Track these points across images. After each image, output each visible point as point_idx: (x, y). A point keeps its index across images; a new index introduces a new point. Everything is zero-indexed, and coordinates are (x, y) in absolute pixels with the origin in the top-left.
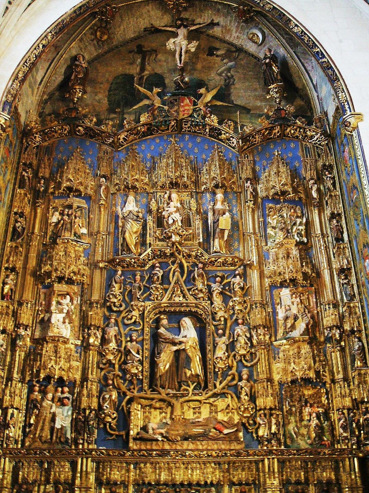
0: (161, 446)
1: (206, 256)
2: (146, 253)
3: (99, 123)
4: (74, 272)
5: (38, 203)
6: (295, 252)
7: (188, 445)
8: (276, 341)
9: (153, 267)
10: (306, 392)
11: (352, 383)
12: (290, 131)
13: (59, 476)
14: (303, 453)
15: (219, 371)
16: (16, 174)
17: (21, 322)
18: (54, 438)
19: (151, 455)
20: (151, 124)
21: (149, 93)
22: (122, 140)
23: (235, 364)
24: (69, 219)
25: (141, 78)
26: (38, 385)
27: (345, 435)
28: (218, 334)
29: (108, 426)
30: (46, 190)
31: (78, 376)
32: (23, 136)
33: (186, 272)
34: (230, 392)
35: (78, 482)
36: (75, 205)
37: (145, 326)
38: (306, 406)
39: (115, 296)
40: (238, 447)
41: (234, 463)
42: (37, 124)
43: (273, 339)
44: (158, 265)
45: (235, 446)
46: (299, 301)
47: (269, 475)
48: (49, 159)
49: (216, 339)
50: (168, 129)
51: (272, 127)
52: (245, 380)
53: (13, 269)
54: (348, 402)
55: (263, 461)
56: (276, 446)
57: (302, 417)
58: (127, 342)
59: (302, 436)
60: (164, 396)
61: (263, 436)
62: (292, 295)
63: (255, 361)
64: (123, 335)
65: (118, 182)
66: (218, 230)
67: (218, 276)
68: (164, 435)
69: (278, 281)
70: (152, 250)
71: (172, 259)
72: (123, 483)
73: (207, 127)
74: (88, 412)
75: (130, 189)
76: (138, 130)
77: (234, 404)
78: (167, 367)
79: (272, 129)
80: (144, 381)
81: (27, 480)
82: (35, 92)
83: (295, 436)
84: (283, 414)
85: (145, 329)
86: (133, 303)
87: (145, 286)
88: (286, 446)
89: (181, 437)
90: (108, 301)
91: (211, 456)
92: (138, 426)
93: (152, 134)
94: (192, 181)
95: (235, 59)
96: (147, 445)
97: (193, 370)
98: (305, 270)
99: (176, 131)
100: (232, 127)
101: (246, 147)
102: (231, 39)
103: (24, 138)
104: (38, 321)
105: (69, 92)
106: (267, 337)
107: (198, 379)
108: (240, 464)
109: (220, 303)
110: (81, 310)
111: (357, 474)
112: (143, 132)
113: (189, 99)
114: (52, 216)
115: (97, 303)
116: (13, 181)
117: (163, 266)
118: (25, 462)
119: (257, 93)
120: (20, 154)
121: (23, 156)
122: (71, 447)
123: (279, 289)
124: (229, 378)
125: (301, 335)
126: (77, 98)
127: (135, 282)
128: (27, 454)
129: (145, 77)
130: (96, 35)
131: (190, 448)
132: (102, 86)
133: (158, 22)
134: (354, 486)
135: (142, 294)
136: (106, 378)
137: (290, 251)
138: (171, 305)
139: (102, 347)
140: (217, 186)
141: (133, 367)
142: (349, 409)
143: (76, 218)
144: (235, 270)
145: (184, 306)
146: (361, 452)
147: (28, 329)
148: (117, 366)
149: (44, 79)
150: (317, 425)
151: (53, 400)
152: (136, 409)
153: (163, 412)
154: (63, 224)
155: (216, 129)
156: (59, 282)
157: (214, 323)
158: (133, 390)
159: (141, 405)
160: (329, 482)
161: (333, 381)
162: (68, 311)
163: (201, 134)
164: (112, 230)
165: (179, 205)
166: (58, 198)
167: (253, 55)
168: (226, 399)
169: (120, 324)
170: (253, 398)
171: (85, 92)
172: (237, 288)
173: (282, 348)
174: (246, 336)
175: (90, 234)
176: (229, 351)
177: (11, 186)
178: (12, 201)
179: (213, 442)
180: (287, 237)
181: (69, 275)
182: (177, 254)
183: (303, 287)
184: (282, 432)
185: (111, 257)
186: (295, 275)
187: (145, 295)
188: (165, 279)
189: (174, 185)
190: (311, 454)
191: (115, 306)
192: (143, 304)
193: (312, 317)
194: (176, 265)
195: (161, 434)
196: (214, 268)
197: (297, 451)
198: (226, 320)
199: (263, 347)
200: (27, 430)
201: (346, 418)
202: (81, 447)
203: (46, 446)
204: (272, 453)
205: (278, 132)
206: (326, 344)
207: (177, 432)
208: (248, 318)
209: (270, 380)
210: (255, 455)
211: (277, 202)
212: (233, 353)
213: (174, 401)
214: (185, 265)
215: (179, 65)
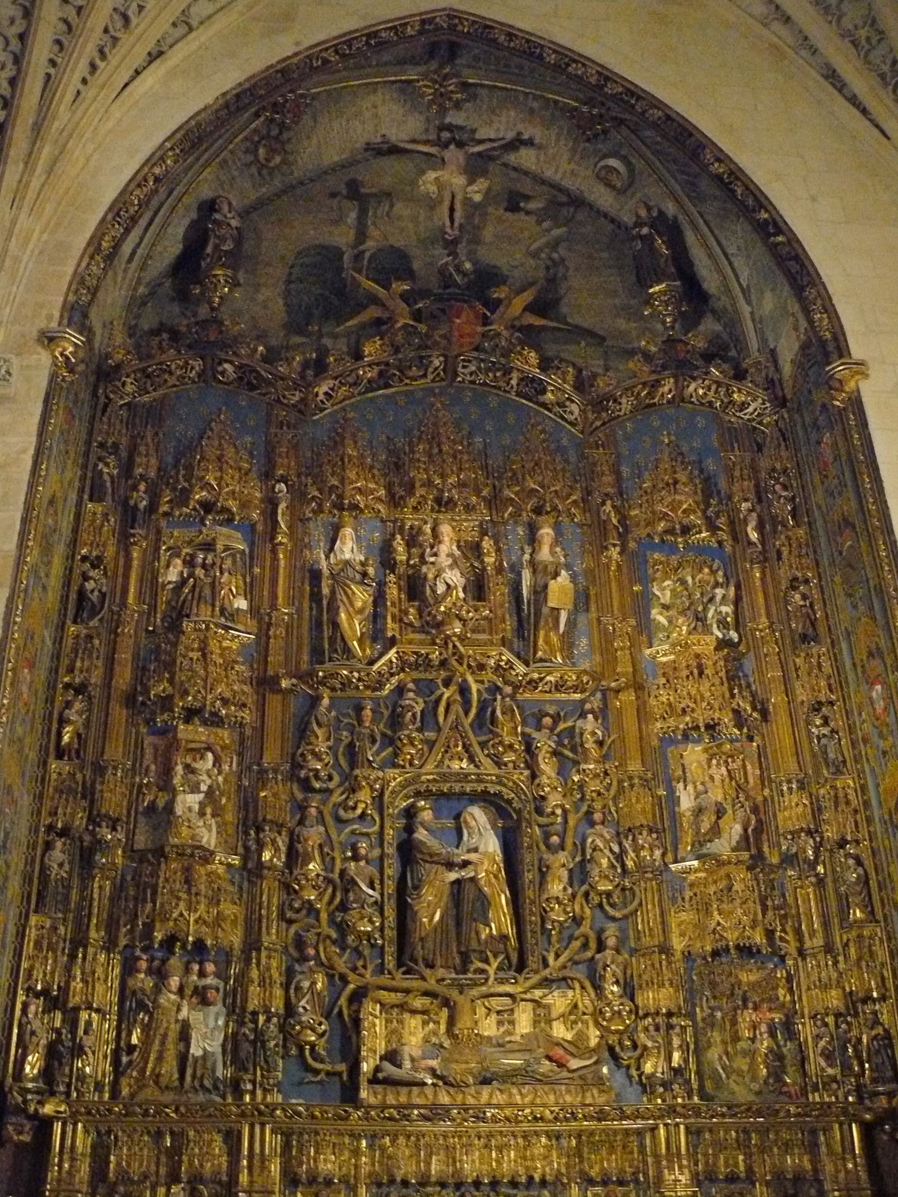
0: (430, 1097)
1: (521, 668)
2: (387, 657)
3: (271, 357)
4: (222, 699)
5: (133, 535)
6: (714, 662)
7: (491, 1096)
8: (676, 861)
9: (400, 690)
10: (744, 977)
11: (841, 958)
12: (695, 390)
13: (201, 1165)
14: (742, 1112)
15: (554, 929)
16: (85, 467)
17: (103, 811)
18: (188, 1078)
19: (407, 1117)
20: (387, 364)
21: (381, 292)
22: (321, 397)
23: (588, 911)
24: (206, 575)
25: (358, 257)
26: (145, 957)
27: (830, 1071)
28: (548, 846)
29: (307, 1053)
30: (152, 508)
31: (235, 939)
32: (98, 379)
33: (475, 704)
34: (578, 976)
35: (244, 1178)
36: (219, 547)
37: (387, 824)
38: (745, 1007)
39: (318, 757)
40: (601, 1100)
41: (592, 1134)
42: (129, 353)
43: (670, 857)
44: (411, 686)
45: (594, 1097)
46: (725, 773)
47: (668, 1161)
48: (157, 434)
49: (545, 856)
50: (425, 376)
51: (658, 381)
52: (612, 949)
53: (81, 689)
54: (834, 999)
55: (654, 1129)
56: (683, 1098)
57: (737, 1032)
58: (346, 859)
59: (739, 1075)
60: (431, 984)
61: (653, 1075)
62: (709, 760)
63: (631, 908)
64: (336, 845)
65: (316, 493)
66: (545, 611)
67: (547, 715)
68: (438, 1072)
69: (677, 728)
70: (397, 653)
71: (443, 674)
72: (344, 1180)
73: (515, 375)
74: (261, 1019)
75: (343, 509)
76: (358, 376)
77: (587, 1002)
78: (437, 917)
79: (656, 384)
80: (387, 949)
81: (127, 1173)
82: (119, 279)
83: (724, 1076)
84: (695, 1025)
85: (386, 831)
86: (357, 772)
87: (384, 735)
88: (703, 1096)
89: (474, 1077)
90: (302, 767)
91: (542, 1119)
92: (375, 1052)
93: (387, 386)
94: (484, 498)
95: (568, 221)
96: (398, 1093)
97: (493, 925)
98: (738, 705)
99: (442, 380)
100: (570, 378)
101: (598, 423)
102: (558, 177)
103: (102, 385)
104: (141, 809)
105: (200, 283)
106: (658, 853)
107: (505, 945)
108: (604, 1138)
109: (553, 775)
110: (239, 786)
111: (858, 1160)
112: (369, 381)
113: (472, 307)
114: (168, 566)
115: (275, 771)
116: (77, 484)
117: (426, 688)
118: (120, 1134)
119: (617, 301)
120: (93, 418)
121: (97, 425)
122: (224, 1097)
123: (681, 746)
124: (576, 944)
125: (734, 850)
126: (221, 298)
127: (359, 725)
128: (126, 1115)
129: (367, 255)
130: (256, 156)
131: (494, 1101)
132: (270, 270)
133: (394, 131)
134: (854, 1186)
135: (378, 753)
136: (300, 943)
137: (704, 661)
138: (444, 777)
139: (291, 873)
140: (538, 511)
141: (362, 918)
142: (838, 1015)
143: (222, 573)
144: (583, 702)
145: (469, 782)
146: (869, 1109)
147: (119, 828)
148: (324, 916)
149: (140, 251)
150: (771, 1050)
151: (181, 991)
152: (372, 1015)
153: (431, 1019)
154: (194, 586)
155: (533, 380)
156: (187, 721)
157: (542, 820)
158: (362, 971)
159: (381, 1005)
160: (798, 1178)
161: (801, 953)
162: (210, 787)
163: (499, 388)
164: (306, 605)
165: (457, 553)
166: (179, 525)
167: (606, 216)
168: (570, 993)
169: (329, 819)
170: (629, 991)
171: (235, 284)
172: (590, 745)
173: (692, 877)
174: (611, 850)
175: (254, 610)
176: (575, 883)
177: (73, 497)
178: (75, 530)
179: (546, 1088)
180: (695, 628)
181: (213, 704)
182: (455, 663)
183: (732, 741)
184: (693, 1066)
185: (304, 667)
186: (717, 715)
187: (383, 754)
188: (428, 718)
189: (443, 504)
190: (759, 1114)
191: (317, 777)
192: (381, 774)
193: (755, 810)
194: (453, 688)
195: (433, 1072)
196: (537, 695)
197: (729, 1108)
198: (565, 812)
199: (650, 875)
200: (125, 1059)
201: (832, 1036)
202: (247, 1098)
203: (168, 1097)
204: (675, 1111)
205: (670, 391)
206: (786, 869)
207: (464, 1066)
208: (613, 809)
209: (665, 949)
210: (637, 1117)
211: (673, 549)
212: (585, 888)
213: (454, 994)
214: (474, 687)
215: (449, 230)
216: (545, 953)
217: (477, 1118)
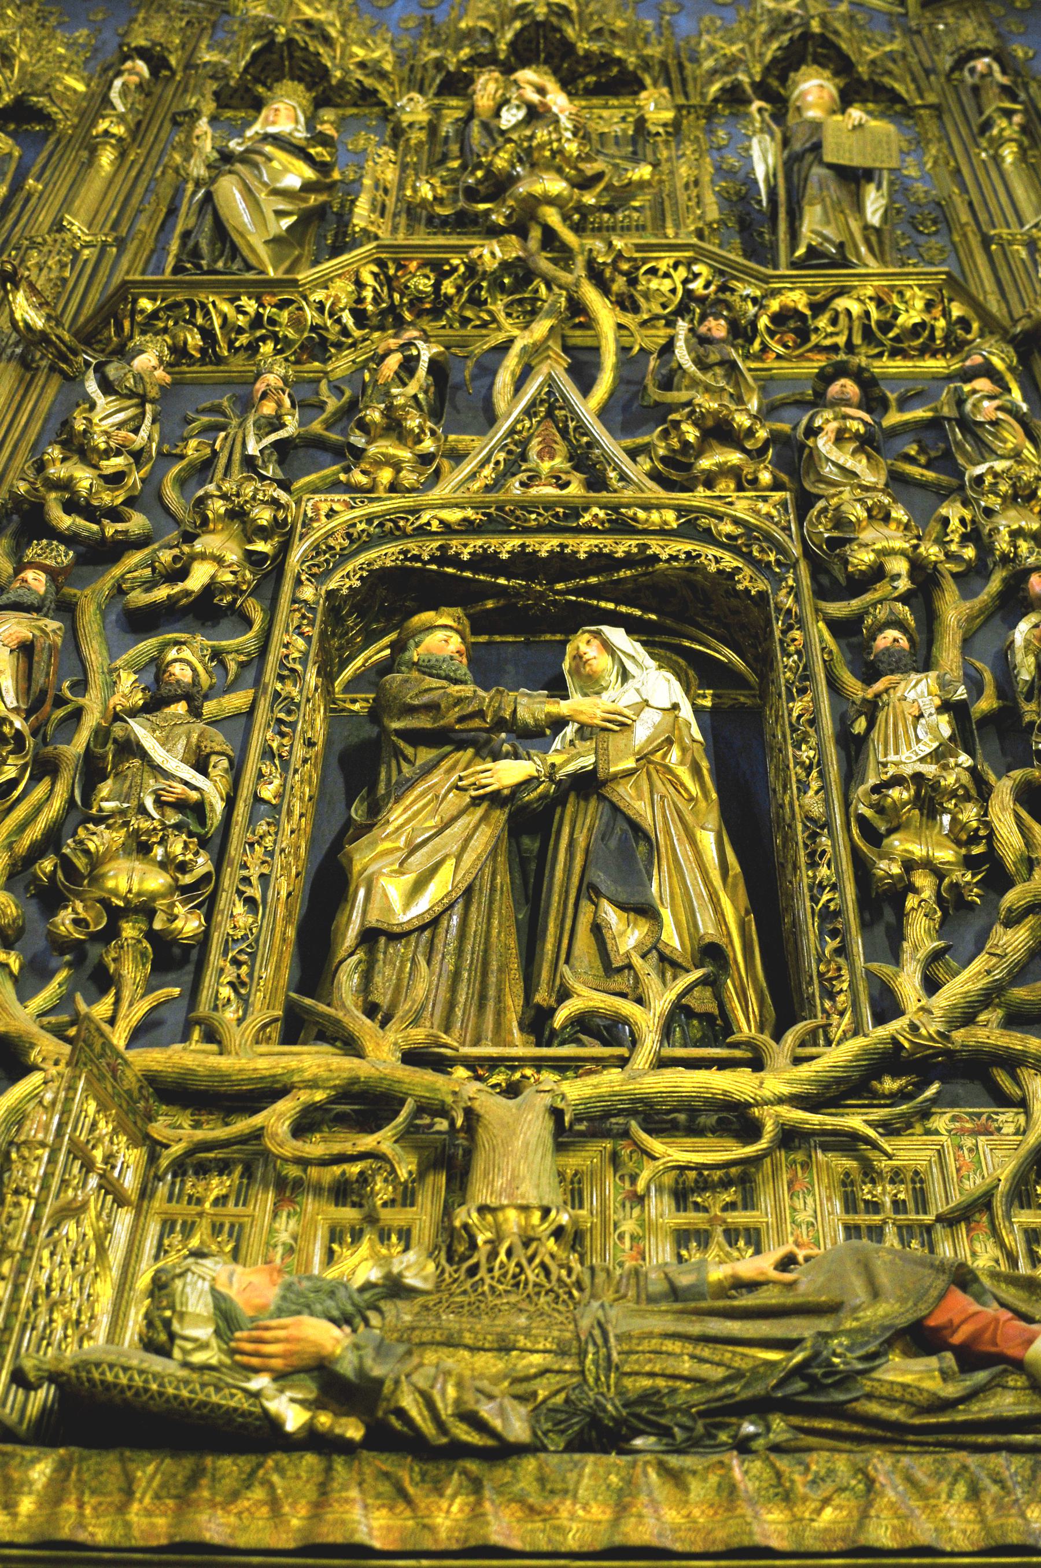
33: (609, 358)
145: (589, 530)
179: (922, 1466)
207: (489, 1363)
216: (883, 969)
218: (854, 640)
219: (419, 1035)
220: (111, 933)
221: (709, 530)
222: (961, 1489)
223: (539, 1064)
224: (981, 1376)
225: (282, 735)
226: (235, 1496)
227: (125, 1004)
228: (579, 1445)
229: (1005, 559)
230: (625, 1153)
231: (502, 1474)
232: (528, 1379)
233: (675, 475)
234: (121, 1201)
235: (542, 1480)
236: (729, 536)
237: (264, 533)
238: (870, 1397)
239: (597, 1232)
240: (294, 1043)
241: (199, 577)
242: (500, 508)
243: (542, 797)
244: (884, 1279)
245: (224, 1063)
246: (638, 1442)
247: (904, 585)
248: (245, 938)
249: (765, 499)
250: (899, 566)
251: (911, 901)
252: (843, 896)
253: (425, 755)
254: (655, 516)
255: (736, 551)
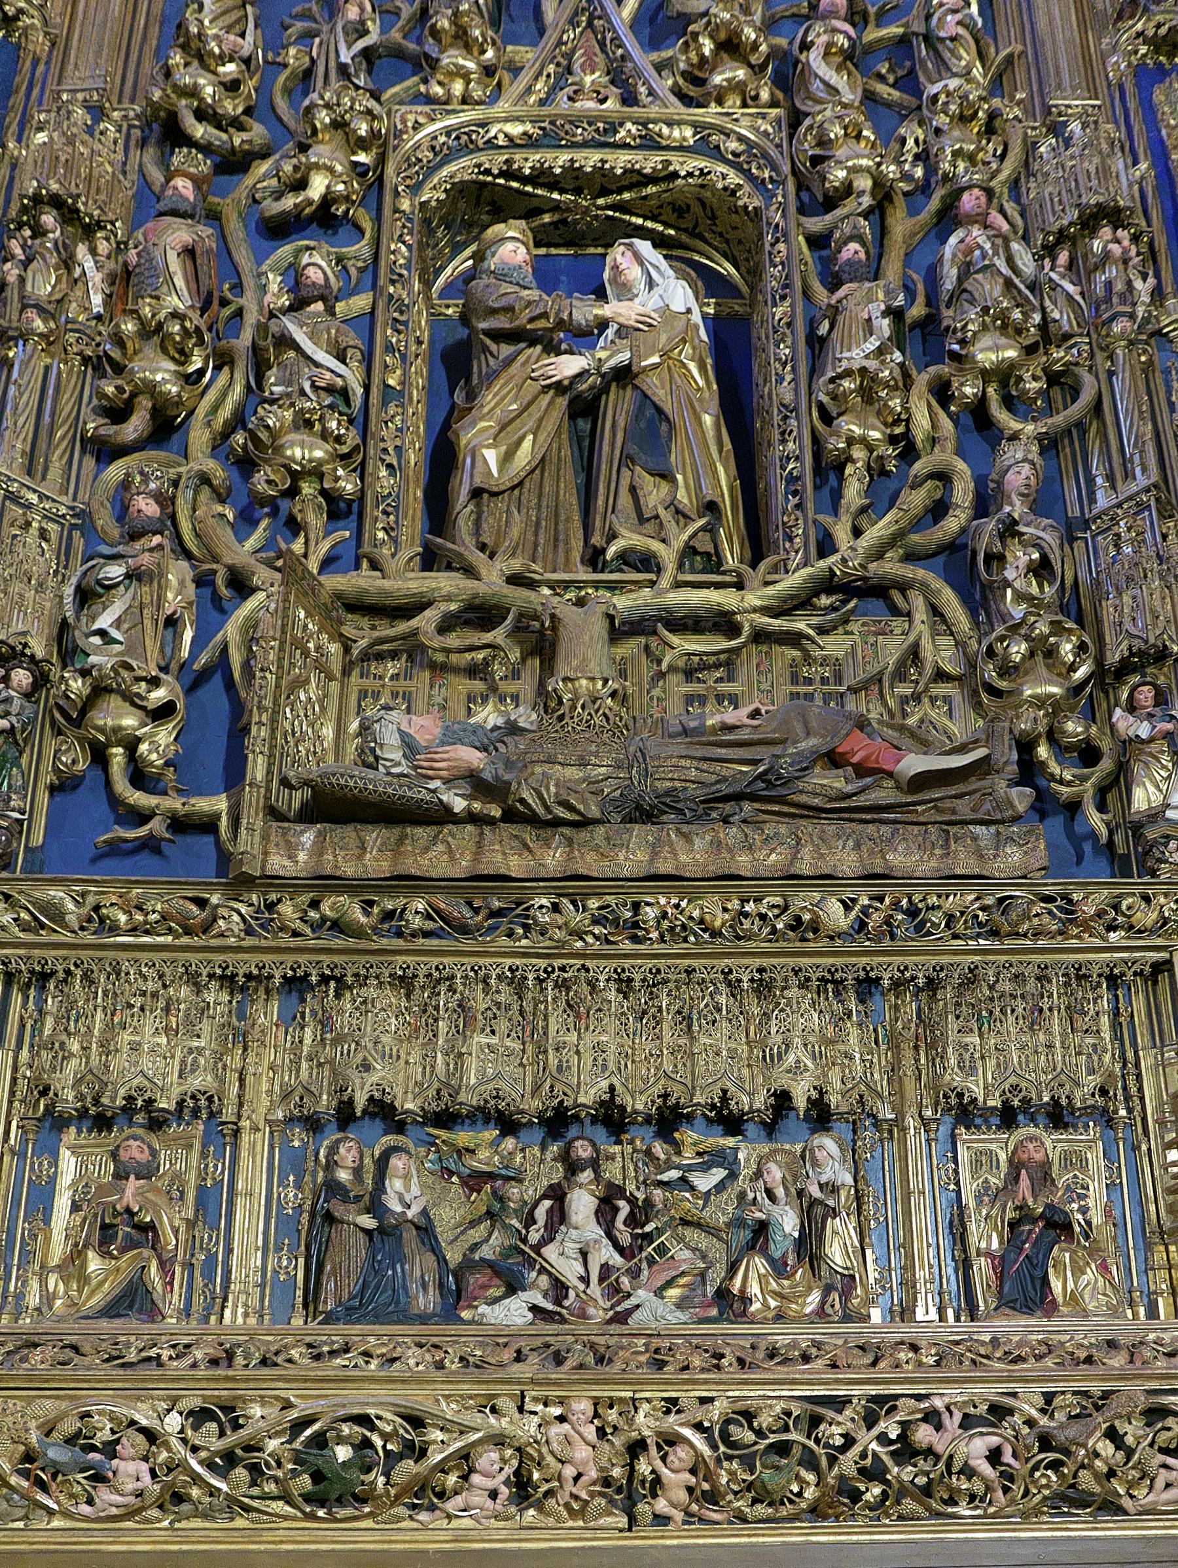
124: (916, 499)
131: (665, 866)
207: (573, 773)
216: (826, 519)
217: (616, 922)
218: (825, 253)
219: (516, 565)
220: (293, 492)
221: (717, 147)
222: (851, 843)
223: (596, 585)
224: (868, 780)
225: (399, 332)
226: (427, 849)
227: (312, 543)
228: (629, 820)
229: (946, 178)
230: (653, 645)
231: (583, 835)
232: (598, 782)
233: (692, 91)
234: (330, 677)
235: (608, 839)
236: (734, 154)
237: (362, 144)
238: (801, 792)
239: (636, 696)
240: (431, 570)
241: (318, 186)
242: (552, 123)
243: (592, 388)
244: (814, 724)
245: (387, 584)
246: (664, 818)
247: (867, 201)
248: (390, 494)
249: (764, 116)
250: (864, 183)
251: (849, 469)
252: (803, 464)
253: (506, 350)
254: (676, 133)
255: (738, 167)
